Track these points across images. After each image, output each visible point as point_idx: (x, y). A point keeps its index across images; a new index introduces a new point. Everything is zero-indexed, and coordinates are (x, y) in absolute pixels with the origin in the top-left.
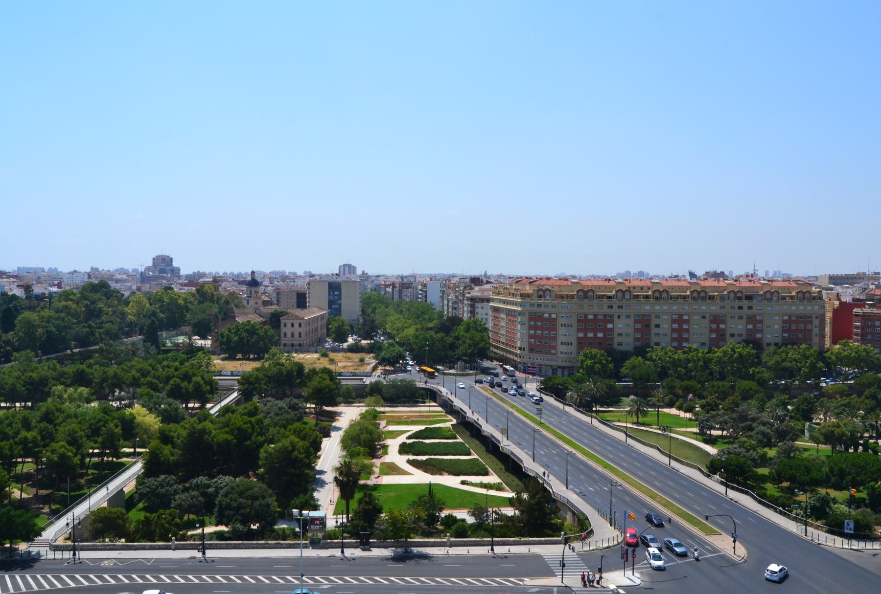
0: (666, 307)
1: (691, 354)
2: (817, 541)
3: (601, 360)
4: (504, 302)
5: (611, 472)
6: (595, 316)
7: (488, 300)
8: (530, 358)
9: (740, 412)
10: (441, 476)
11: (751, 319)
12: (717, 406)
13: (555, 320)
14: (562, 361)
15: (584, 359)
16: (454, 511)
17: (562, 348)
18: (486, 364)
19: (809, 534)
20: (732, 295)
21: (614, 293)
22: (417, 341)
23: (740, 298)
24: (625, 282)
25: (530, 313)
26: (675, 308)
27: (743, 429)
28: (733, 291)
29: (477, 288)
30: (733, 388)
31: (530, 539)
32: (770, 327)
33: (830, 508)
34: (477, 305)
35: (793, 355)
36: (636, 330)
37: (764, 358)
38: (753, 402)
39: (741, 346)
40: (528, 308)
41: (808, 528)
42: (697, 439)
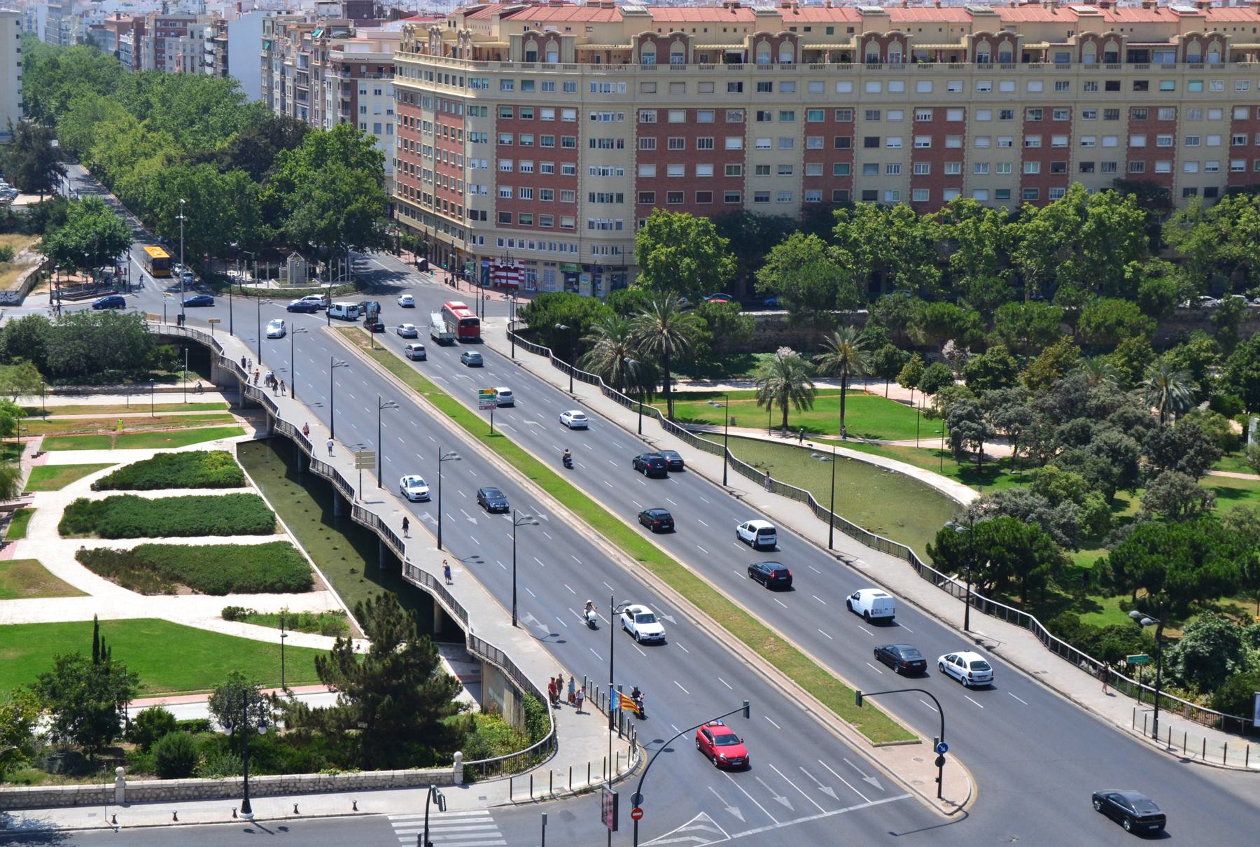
0: (897, 86)
1: (960, 225)
2: (1180, 753)
3: (698, 246)
4: (432, 75)
5: (656, 571)
6: (691, 113)
7: (392, 70)
8: (501, 243)
9: (1068, 391)
10: (171, 597)
11: (1143, 120)
12: (1010, 374)
13: (573, 127)
14: (594, 250)
15: (650, 242)
16: (169, 700)
17: (594, 212)
18: (379, 261)
19: (1162, 733)
20: (1090, 48)
21: (746, 44)
22: (164, 195)
23: (1113, 58)
24: (781, 11)
25: (500, 107)
26: (925, 87)
27: (1065, 438)
28: (1094, 37)
29: (362, 33)
30: (1071, 319)
31: (363, 774)
32: (1196, 141)
33: (1239, 659)
34: (362, 84)
35: (1250, 221)
36: (810, 156)
37: (1171, 231)
38: (1112, 361)
39: (1106, 198)
40: (495, 91)
41: (1162, 713)
42: (942, 471)
